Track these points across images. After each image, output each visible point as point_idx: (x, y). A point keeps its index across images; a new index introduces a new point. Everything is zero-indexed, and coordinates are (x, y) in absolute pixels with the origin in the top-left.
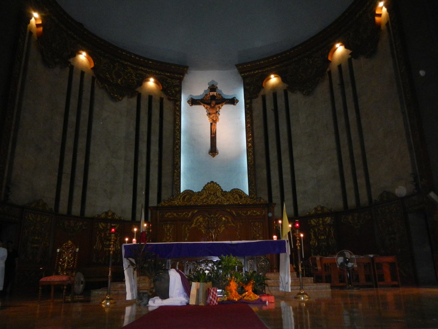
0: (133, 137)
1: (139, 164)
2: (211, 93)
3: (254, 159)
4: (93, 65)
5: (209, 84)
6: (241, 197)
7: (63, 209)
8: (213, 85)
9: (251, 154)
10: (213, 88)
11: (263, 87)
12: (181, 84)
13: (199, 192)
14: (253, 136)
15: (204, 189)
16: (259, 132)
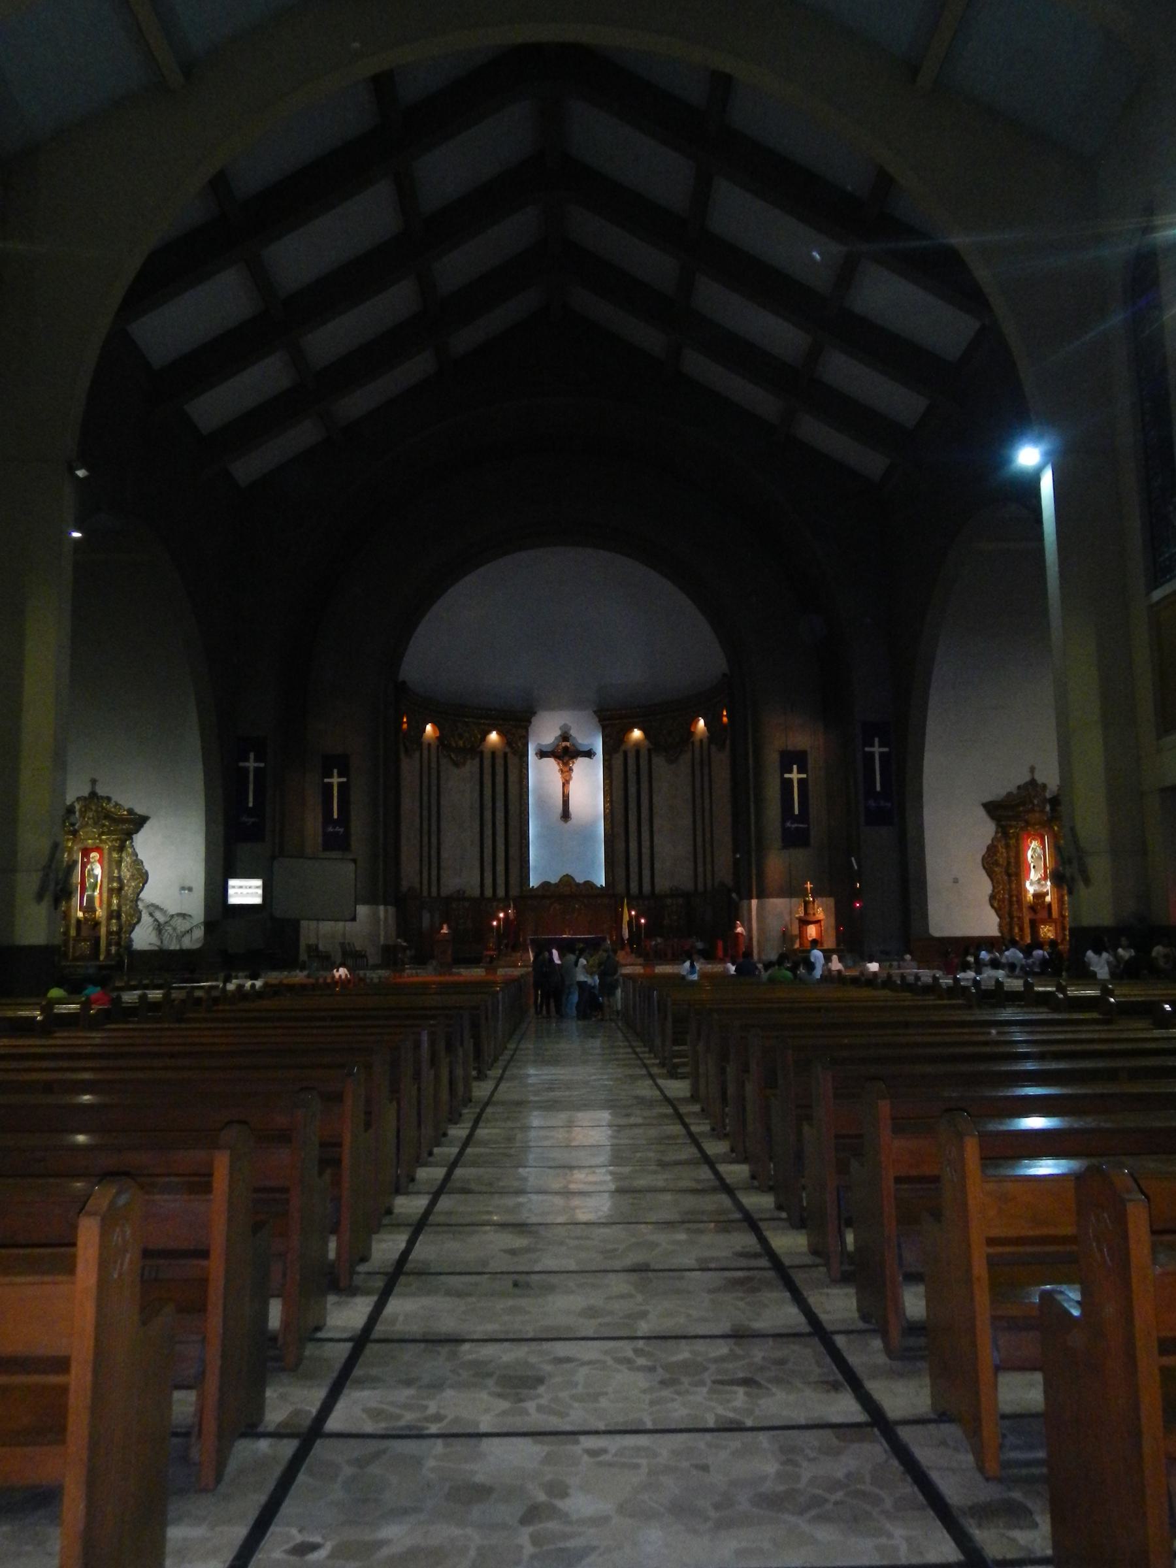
0: (477, 805)
1: (485, 836)
2: (564, 744)
3: (612, 828)
4: (438, 735)
5: (560, 728)
6: (592, 888)
7: (425, 894)
8: (566, 732)
9: (608, 822)
10: (565, 737)
11: (624, 742)
12: (527, 732)
13: (556, 884)
14: (611, 802)
15: (561, 880)
16: (618, 794)
